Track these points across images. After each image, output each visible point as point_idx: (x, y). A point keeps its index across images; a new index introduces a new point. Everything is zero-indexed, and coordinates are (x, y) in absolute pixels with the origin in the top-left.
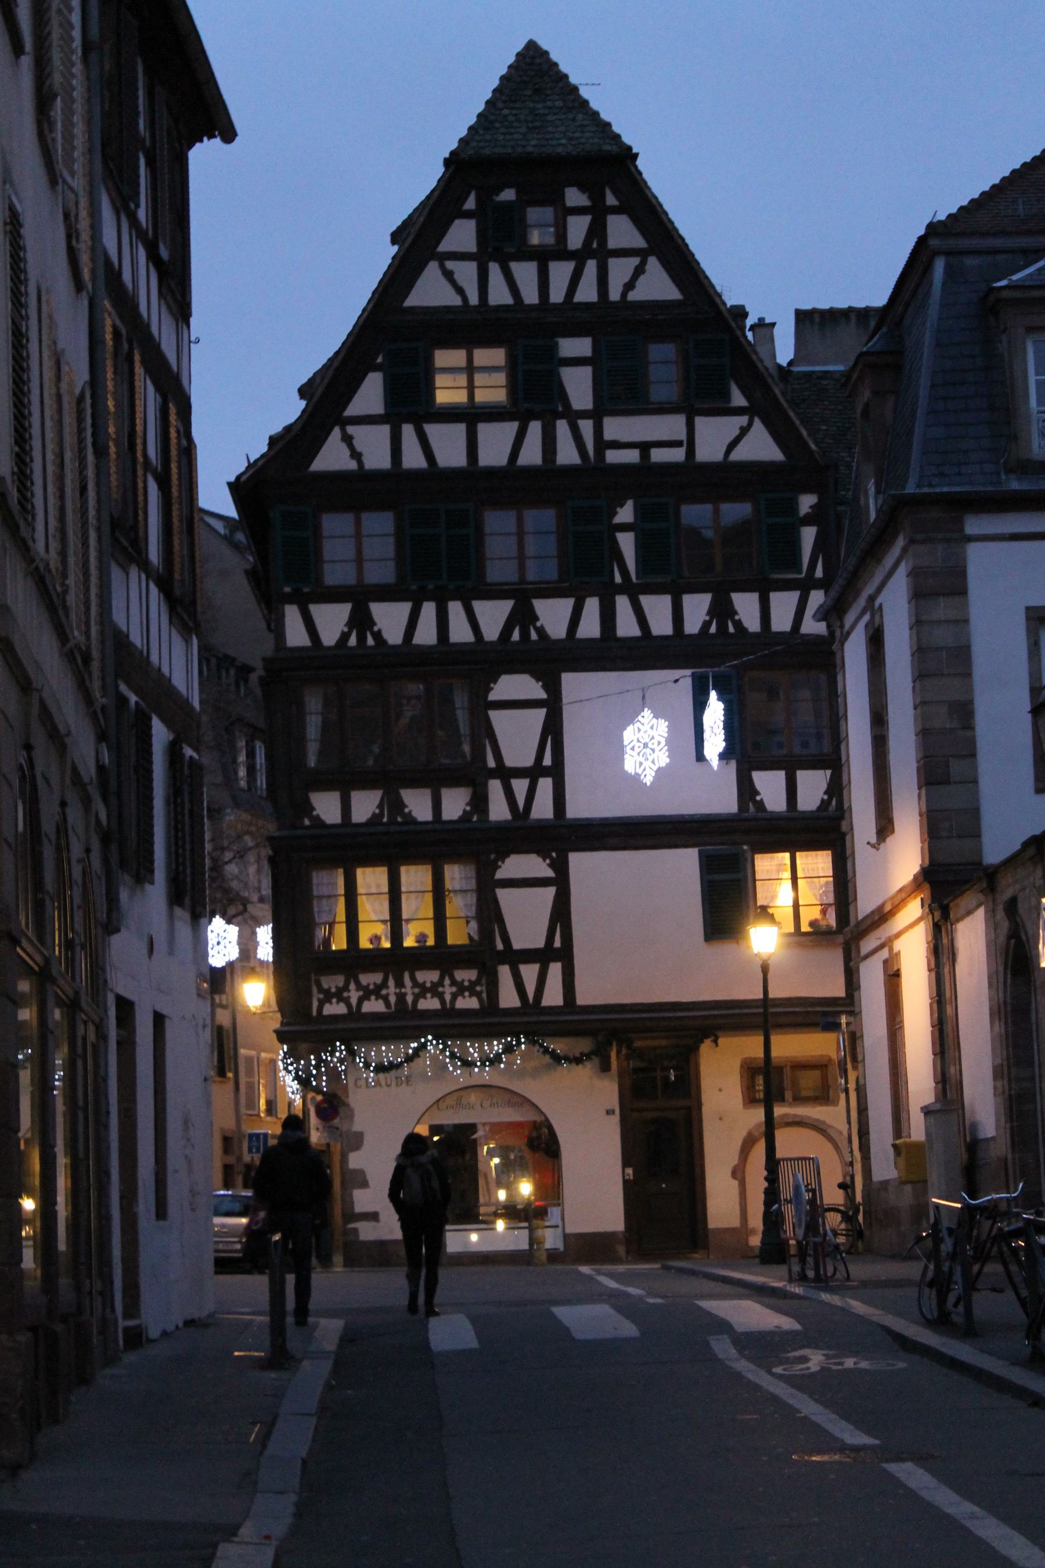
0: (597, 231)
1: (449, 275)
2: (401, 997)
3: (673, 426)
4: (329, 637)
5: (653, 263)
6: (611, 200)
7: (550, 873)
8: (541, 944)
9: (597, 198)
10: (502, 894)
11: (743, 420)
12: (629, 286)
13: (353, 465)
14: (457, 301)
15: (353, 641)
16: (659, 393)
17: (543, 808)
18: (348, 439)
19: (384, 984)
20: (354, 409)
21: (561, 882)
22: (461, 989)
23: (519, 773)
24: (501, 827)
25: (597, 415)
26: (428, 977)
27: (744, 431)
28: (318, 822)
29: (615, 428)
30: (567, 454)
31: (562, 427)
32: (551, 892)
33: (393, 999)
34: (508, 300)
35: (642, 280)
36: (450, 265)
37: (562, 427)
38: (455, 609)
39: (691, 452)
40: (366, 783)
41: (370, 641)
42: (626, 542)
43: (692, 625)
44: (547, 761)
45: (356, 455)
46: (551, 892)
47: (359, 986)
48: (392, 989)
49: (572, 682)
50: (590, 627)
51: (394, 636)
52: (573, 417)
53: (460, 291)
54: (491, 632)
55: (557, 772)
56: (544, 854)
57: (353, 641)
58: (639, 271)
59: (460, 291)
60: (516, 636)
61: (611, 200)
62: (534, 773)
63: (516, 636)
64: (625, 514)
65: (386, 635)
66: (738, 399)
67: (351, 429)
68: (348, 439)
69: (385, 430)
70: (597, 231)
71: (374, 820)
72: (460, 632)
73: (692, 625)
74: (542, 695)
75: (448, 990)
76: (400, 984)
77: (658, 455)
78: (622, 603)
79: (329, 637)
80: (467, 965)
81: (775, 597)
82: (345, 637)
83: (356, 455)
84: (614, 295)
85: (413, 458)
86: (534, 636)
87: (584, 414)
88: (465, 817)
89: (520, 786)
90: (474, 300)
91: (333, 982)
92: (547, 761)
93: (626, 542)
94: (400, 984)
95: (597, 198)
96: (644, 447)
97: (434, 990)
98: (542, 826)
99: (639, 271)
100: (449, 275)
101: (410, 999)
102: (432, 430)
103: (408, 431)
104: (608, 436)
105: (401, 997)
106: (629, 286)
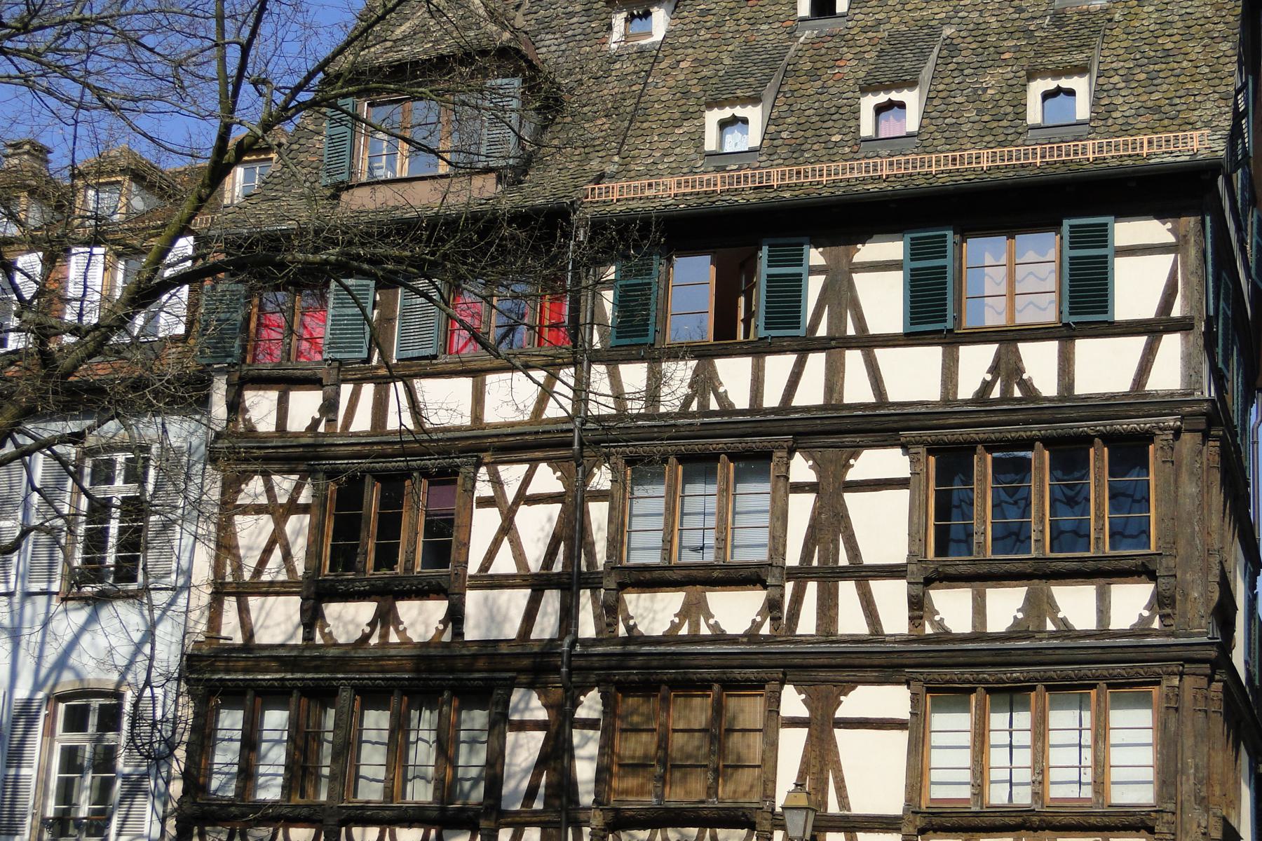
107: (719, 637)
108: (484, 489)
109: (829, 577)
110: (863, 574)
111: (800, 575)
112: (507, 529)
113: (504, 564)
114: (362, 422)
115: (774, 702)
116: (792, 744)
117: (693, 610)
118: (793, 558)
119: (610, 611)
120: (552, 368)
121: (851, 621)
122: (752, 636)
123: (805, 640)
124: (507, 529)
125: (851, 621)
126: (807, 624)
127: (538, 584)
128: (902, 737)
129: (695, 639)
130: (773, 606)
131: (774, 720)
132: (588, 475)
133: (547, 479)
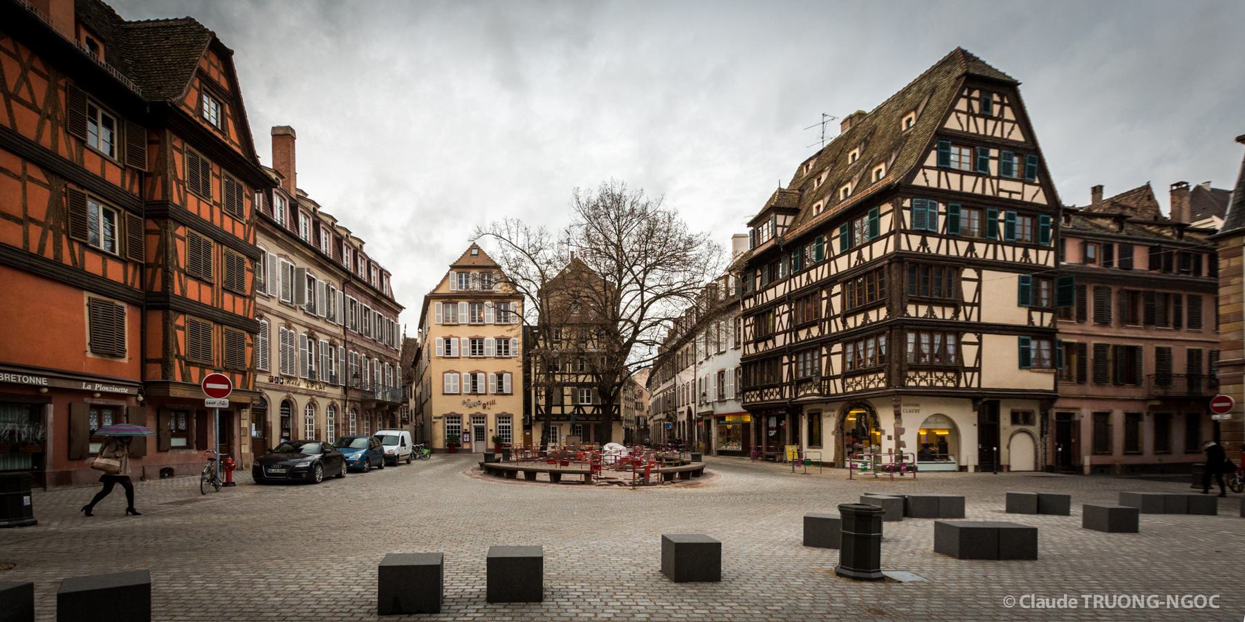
0: (1002, 111)
1: (958, 118)
2: (931, 381)
3: (1016, 186)
4: (914, 249)
5: (1016, 126)
6: (1006, 101)
7: (977, 341)
8: (973, 366)
9: (1002, 99)
10: (964, 347)
11: (1037, 188)
12: (1010, 134)
13: (925, 184)
14: (960, 129)
15: (921, 250)
16: (1015, 175)
17: (974, 319)
18: (925, 174)
19: (926, 376)
20: (927, 163)
21: (980, 344)
22: (949, 379)
23: (968, 304)
24: (961, 323)
25: (999, 178)
26: (940, 374)
27: (1038, 192)
28: (909, 316)
29: (1004, 184)
30: (989, 192)
31: (988, 181)
32: (977, 347)
33: (929, 382)
34: (975, 132)
35: (1013, 132)
36: (959, 114)
37: (988, 181)
38: (952, 242)
39: (1023, 197)
40: (923, 303)
41: (926, 251)
42: (1001, 225)
43: (1018, 259)
44: (976, 301)
45: (927, 181)
46: (977, 347)
47: (919, 377)
48: (929, 378)
49: (985, 273)
50: (990, 256)
51: (933, 251)
52: (992, 178)
53: (961, 125)
54: (962, 254)
55: (979, 305)
56: (975, 333)
57: (921, 250)
58: (1013, 129)
59: (961, 125)
60: (969, 255)
61: (1006, 101)
62: (972, 305)
63: (969, 255)
64: (1002, 216)
65: (931, 249)
66: (1037, 181)
67: (926, 171)
68: (925, 174)
69: (936, 173)
70: (1002, 111)
71: (925, 317)
72: (953, 252)
73: (1018, 259)
74: (976, 277)
75: (945, 380)
76: (931, 377)
77: (1015, 197)
78: (999, 247)
79: (914, 249)
80: (951, 371)
81: (1040, 252)
82: (919, 248)
83: (927, 181)
84: (1005, 136)
85: (944, 186)
86: (974, 256)
87: (994, 178)
88: (952, 318)
89: (968, 309)
90: (965, 130)
91: (911, 374)
92: (976, 301)
93: (1001, 225)
94: (931, 377)
95: (1002, 99)
96: (1011, 193)
97: (941, 379)
98: (974, 324)
99: (1013, 129)
100: (958, 118)
101: (934, 382)
102: (950, 175)
103: (943, 174)
104: (1001, 187)
105: (931, 381)
106: (1010, 134)
107: (813, 338)
108: (777, 313)
109: (829, 319)
110: (835, 317)
111: (824, 320)
112: (781, 321)
113: (780, 329)
114: (760, 303)
115: (821, 351)
116: (824, 359)
117: (809, 332)
118: (823, 317)
119: (797, 336)
120: (785, 281)
121: (834, 330)
122: (818, 337)
123: (827, 335)
124: (781, 321)
125: (834, 330)
126: (826, 332)
127: (785, 332)
128: (840, 355)
129: (809, 339)
130: (820, 328)
131: (821, 356)
132: (791, 306)
133: (786, 308)
